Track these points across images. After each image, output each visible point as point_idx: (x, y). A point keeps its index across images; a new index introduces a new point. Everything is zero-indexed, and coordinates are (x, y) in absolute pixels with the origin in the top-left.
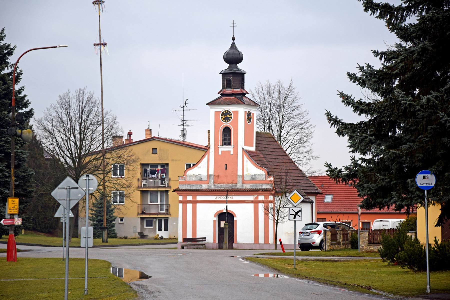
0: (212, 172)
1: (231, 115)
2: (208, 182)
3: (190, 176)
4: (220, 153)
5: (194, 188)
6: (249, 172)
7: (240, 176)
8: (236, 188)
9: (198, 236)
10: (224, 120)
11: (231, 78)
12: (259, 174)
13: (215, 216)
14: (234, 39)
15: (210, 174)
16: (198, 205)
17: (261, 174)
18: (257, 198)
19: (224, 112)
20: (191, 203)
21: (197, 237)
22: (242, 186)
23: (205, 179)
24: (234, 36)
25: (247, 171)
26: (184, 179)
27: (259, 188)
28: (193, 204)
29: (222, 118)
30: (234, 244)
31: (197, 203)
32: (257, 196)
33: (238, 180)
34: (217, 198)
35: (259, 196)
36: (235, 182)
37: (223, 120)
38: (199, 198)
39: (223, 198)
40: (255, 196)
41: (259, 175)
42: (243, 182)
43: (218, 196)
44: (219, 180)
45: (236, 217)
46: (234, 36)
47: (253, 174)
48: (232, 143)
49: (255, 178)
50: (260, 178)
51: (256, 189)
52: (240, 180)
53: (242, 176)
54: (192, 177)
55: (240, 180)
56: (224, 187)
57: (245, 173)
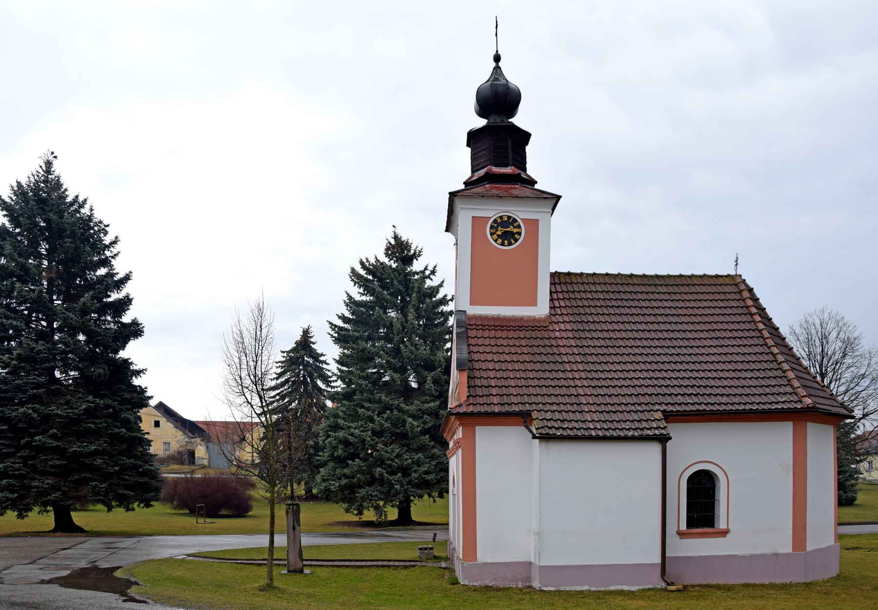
1: (519, 226)
10: (500, 241)
14: (497, 58)
19: (499, 221)
24: (497, 51)
29: (492, 234)
37: (496, 241)
46: (497, 51)
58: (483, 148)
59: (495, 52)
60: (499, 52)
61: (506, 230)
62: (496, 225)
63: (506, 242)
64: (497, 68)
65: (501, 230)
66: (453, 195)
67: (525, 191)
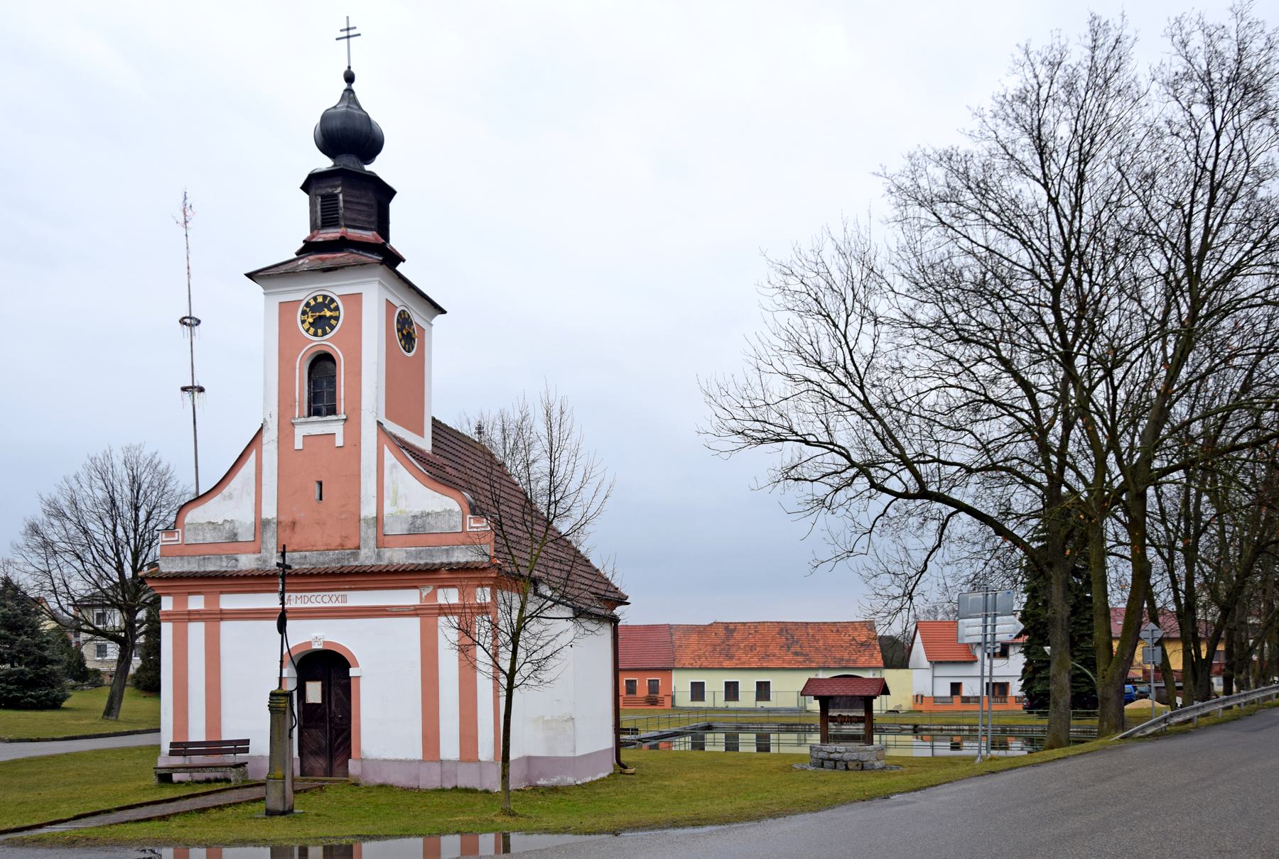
0: (270, 512)
1: (337, 308)
2: (256, 545)
3: (197, 527)
4: (298, 444)
5: (211, 567)
6: (403, 505)
7: (372, 522)
8: (357, 563)
9: (227, 736)
10: (312, 330)
11: (339, 189)
12: (438, 510)
14: (349, 78)
16: (226, 627)
17: (445, 511)
18: (434, 595)
19: (313, 303)
21: (224, 738)
22: (379, 556)
23: (246, 535)
24: (349, 67)
25: (395, 503)
26: (177, 537)
27: (438, 561)
29: (303, 322)
30: (350, 761)
31: (222, 619)
32: (431, 589)
33: (362, 534)
35: (440, 592)
36: (351, 543)
37: (307, 331)
38: (229, 602)
39: (309, 600)
40: (426, 592)
41: (438, 514)
42: (382, 541)
45: (357, 665)
46: (349, 67)
47: (417, 510)
48: (341, 406)
52: (369, 534)
53: (378, 520)
54: (203, 530)
55: (369, 534)
56: (314, 561)
57: (388, 509)
58: (363, 201)
59: (346, 68)
60: (352, 69)
62: (308, 310)
63: (320, 331)
64: (349, 91)
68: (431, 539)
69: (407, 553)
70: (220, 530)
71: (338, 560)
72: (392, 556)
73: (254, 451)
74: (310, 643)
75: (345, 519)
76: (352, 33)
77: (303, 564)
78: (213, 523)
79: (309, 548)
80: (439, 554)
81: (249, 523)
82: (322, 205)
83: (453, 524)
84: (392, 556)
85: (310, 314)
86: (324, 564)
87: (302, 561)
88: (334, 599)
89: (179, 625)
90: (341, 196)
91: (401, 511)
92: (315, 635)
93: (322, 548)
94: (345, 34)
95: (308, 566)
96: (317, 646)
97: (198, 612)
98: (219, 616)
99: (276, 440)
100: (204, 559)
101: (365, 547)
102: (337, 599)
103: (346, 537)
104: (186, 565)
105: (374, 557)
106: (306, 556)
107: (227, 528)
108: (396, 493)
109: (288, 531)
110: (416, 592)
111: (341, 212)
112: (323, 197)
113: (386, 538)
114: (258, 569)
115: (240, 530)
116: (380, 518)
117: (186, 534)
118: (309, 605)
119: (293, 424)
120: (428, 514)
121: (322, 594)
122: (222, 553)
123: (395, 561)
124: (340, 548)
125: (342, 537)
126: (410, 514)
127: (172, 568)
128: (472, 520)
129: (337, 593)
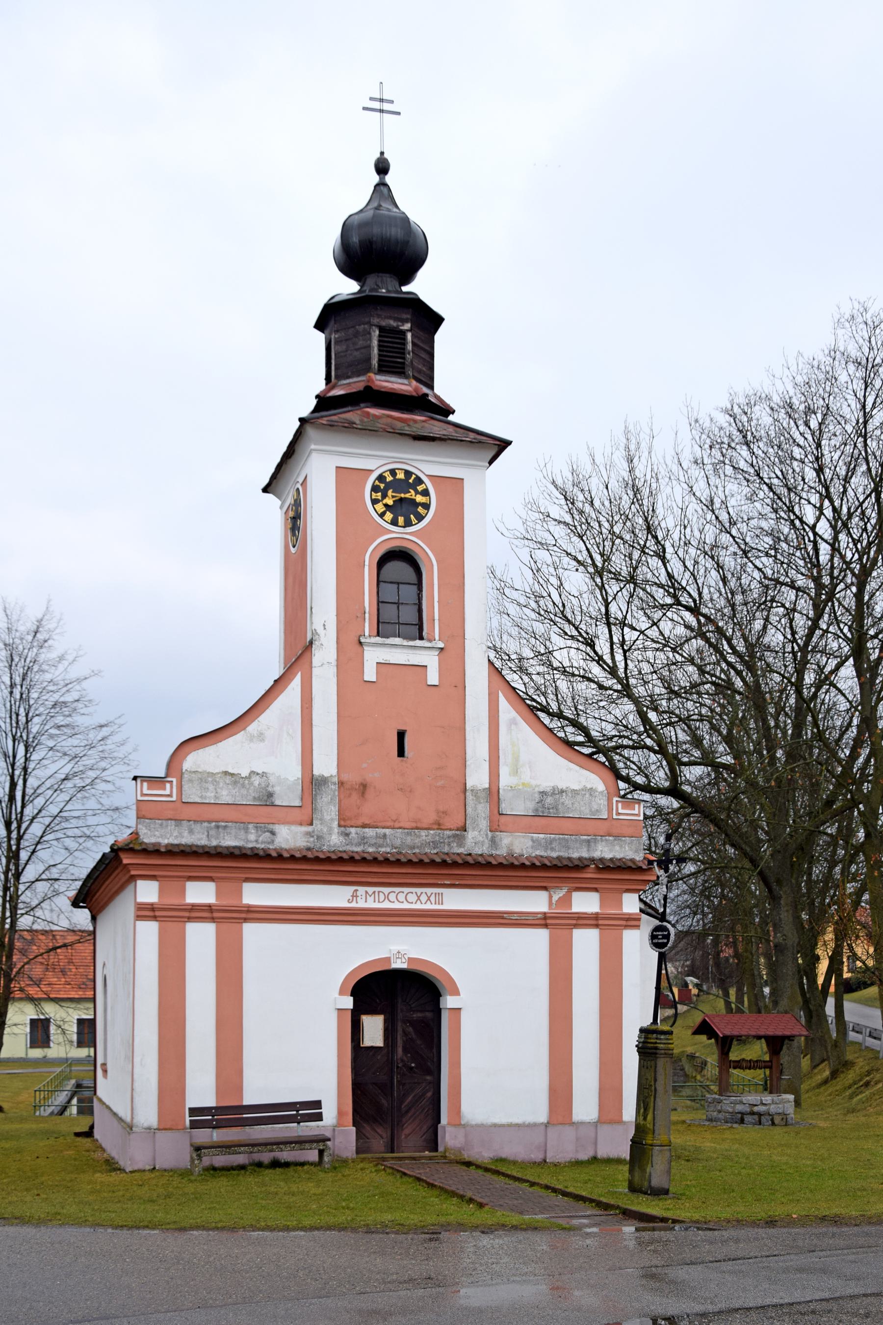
1: (426, 493)
3: (205, 778)
4: (370, 674)
5: (229, 841)
6: (526, 776)
7: (483, 795)
8: (461, 850)
10: (389, 516)
11: (407, 326)
12: (576, 787)
13: (342, 992)
14: (382, 168)
15: (316, 772)
16: (251, 931)
17: (585, 789)
18: (567, 900)
19: (389, 478)
20: (213, 920)
21: (246, 1102)
22: (493, 842)
24: (382, 153)
25: (515, 772)
26: (169, 790)
27: (575, 855)
28: (225, 926)
29: (374, 502)
31: (246, 920)
33: (469, 810)
34: (355, 896)
37: (382, 515)
39: (387, 897)
40: (557, 895)
41: (575, 792)
43: (362, 890)
44: (369, 809)
46: (382, 153)
47: (546, 784)
49: (556, 807)
50: (581, 808)
51: (559, 858)
52: (479, 812)
53: (493, 794)
54: (215, 783)
55: (479, 812)
56: (398, 842)
57: (505, 780)
59: (378, 155)
60: (386, 156)
61: (403, 495)
63: (401, 520)
65: (393, 497)
66: (302, 420)
67: (436, 428)
68: (567, 825)
69: (533, 841)
70: (243, 786)
71: (435, 844)
72: (512, 844)
73: (299, 674)
74: (388, 960)
75: (443, 787)
76: (386, 107)
77: (381, 846)
78: (232, 775)
79: (389, 824)
80: (578, 845)
81: (292, 779)
82: (379, 341)
83: (595, 807)
84: (512, 844)
85: (390, 493)
86: (414, 848)
87: (381, 841)
88: (424, 898)
89: (171, 926)
90: (409, 336)
91: (523, 784)
92: (395, 948)
93: (407, 825)
94: (377, 105)
95: (388, 850)
96: (399, 964)
97: (209, 908)
98: (243, 915)
99: (334, 663)
100: (218, 827)
101: (474, 829)
102: (429, 899)
103: (445, 813)
104: (186, 834)
105: (486, 845)
106: (385, 836)
107: (256, 783)
108: (516, 759)
109: (355, 796)
110: (543, 895)
111: (409, 357)
112: (382, 329)
113: (503, 819)
114: (309, 849)
115: (277, 789)
116: (494, 790)
117: (186, 787)
118: (386, 905)
119: (360, 643)
120: (562, 791)
121: (406, 890)
122: (246, 819)
123: (517, 851)
124: (436, 827)
125: (438, 812)
126: (537, 789)
127: (162, 836)
128: (620, 805)
129: (429, 891)
